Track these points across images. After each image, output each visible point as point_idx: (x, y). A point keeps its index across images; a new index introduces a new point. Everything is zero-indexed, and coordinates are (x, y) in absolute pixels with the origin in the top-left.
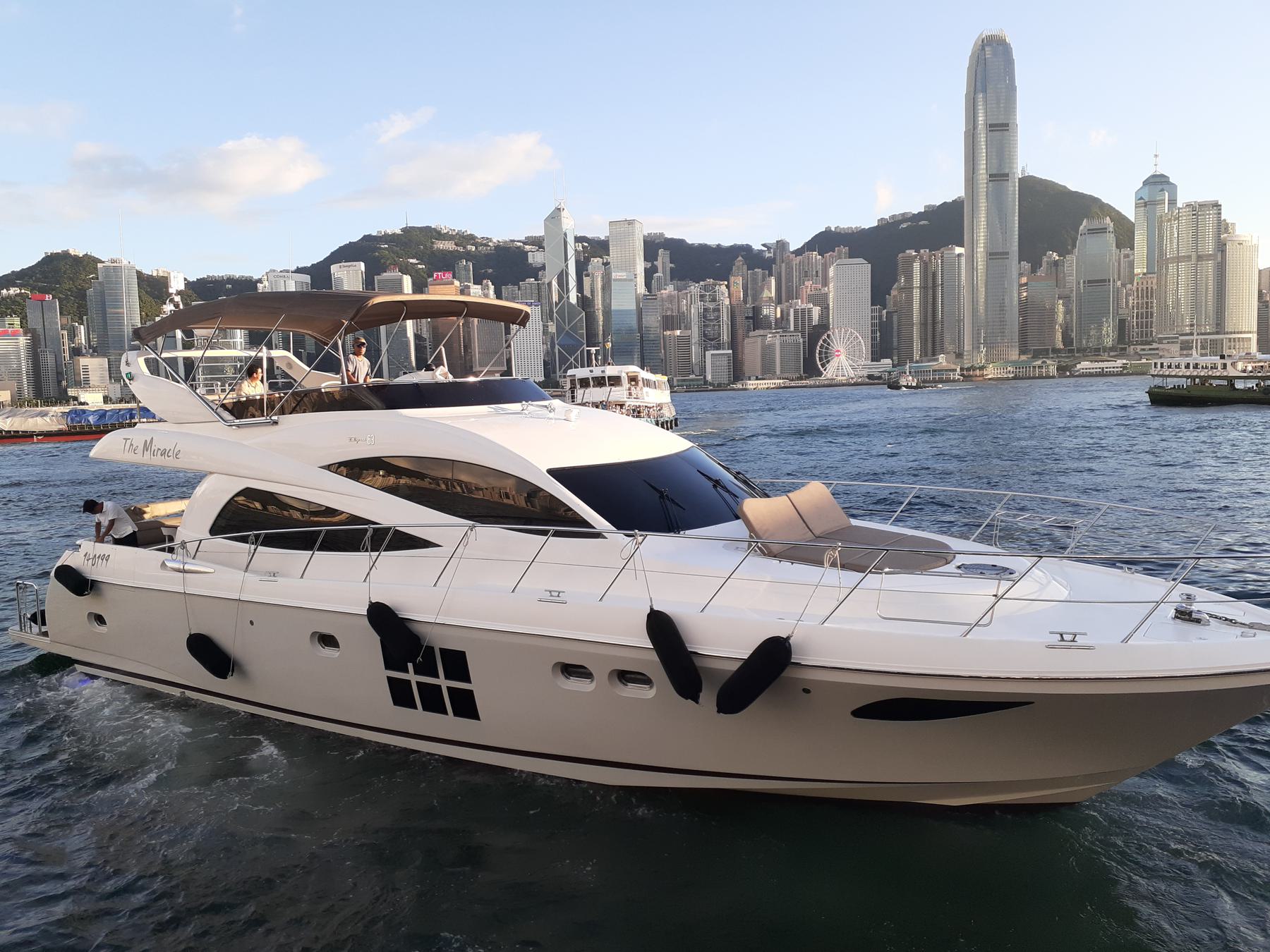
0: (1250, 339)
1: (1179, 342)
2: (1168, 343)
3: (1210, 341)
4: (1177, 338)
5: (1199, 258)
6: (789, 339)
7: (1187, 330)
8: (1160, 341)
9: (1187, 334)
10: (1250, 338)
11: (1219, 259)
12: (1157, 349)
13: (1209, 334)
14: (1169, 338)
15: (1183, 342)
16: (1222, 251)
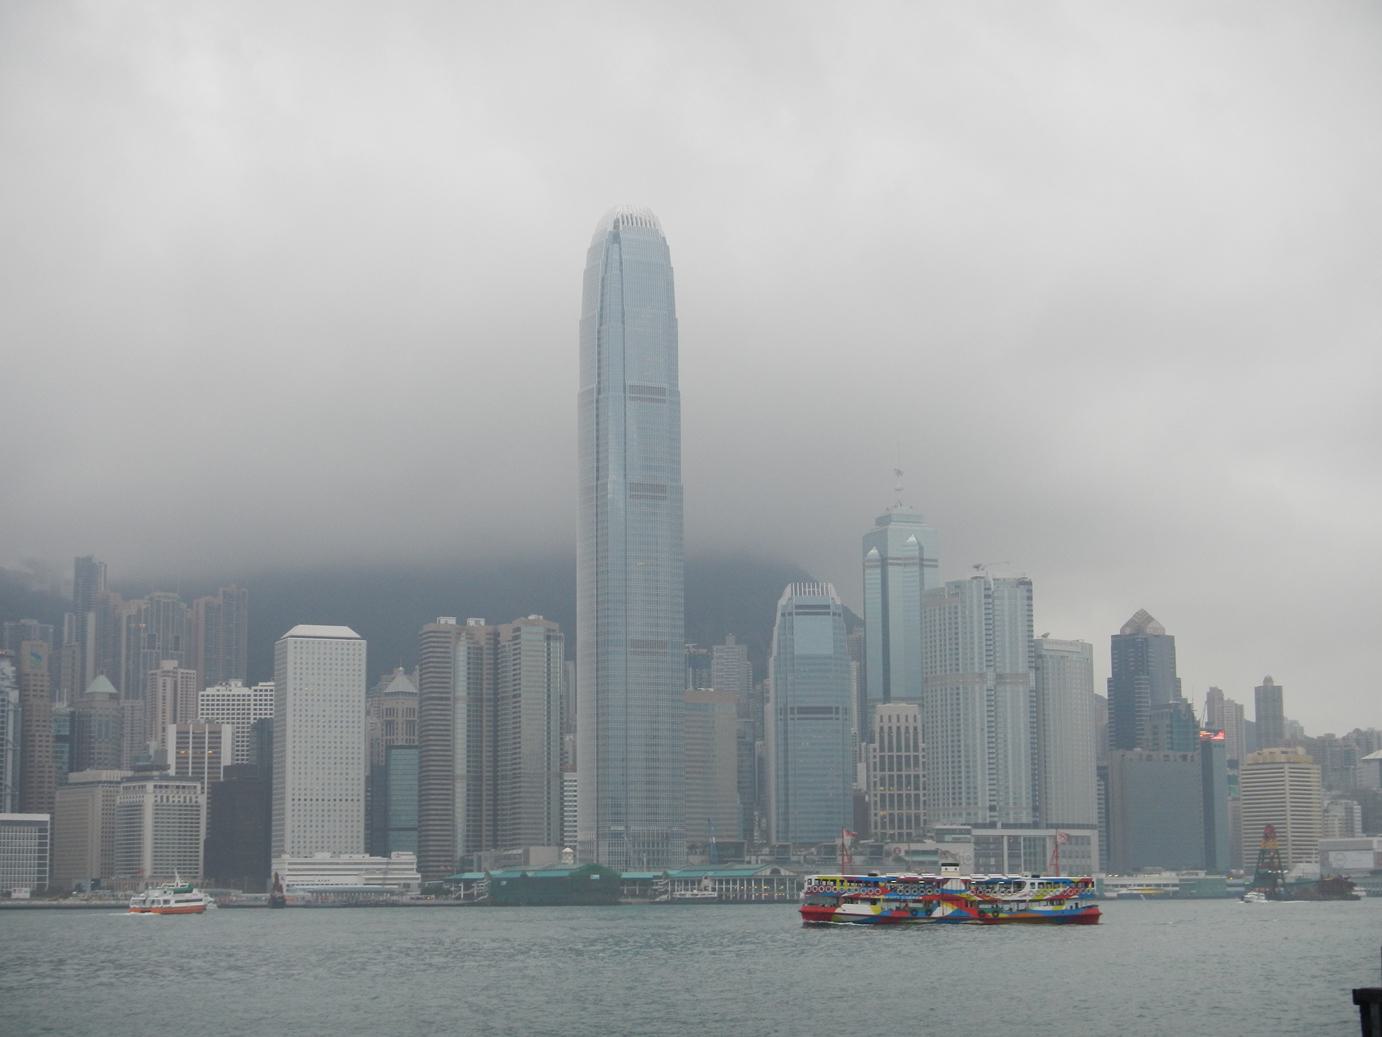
0: (1086, 840)
1: (973, 840)
2: (956, 841)
3: (1024, 840)
4: (968, 832)
5: (1000, 678)
6: (176, 798)
7: (984, 815)
8: (940, 836)
9: (984, 826)
10: (1088, 838)
11: (1033, 684)
12: (935, 852)
13: (1022, 826)
14: (953, 832)
15: (979, 841)
16: (1037, 669)
